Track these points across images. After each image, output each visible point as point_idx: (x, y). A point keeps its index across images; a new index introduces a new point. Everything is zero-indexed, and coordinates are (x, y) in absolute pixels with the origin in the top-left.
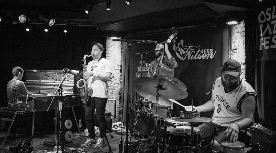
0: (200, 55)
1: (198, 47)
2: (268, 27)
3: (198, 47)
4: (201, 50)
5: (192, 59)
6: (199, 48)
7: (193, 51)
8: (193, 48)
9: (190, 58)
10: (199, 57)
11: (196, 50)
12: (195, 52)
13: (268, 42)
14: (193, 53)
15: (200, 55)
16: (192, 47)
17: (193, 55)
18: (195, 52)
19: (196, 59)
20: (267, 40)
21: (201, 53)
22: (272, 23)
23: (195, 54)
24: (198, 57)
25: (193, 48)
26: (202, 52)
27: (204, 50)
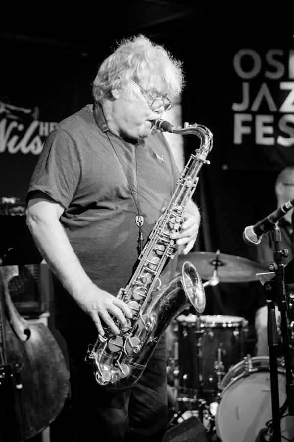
0: (37, 139)
1: (32, 113)
2: (264, 90)
3: (32, 113)
4: (42, 124)
5: (12, 150)
6: (36, 115)
7: (14, 124)
8: (13, 112)
9: (7, 148)
10: (36, 145)
11: (26, 121)
12: (21, 127)
13: (270, 130)
14: (15, 132)
15: (37, 139)
16: (13, 107)
17: (15, 138)
18: (21, 127)
19: (25, 151)
20: (265, 124)
21: (41, 133)
22: (284, 86)
23: (21, 135)
24: (32, 147)
25: (13, 112)
26: (44, 129)
27: (52, 124)
